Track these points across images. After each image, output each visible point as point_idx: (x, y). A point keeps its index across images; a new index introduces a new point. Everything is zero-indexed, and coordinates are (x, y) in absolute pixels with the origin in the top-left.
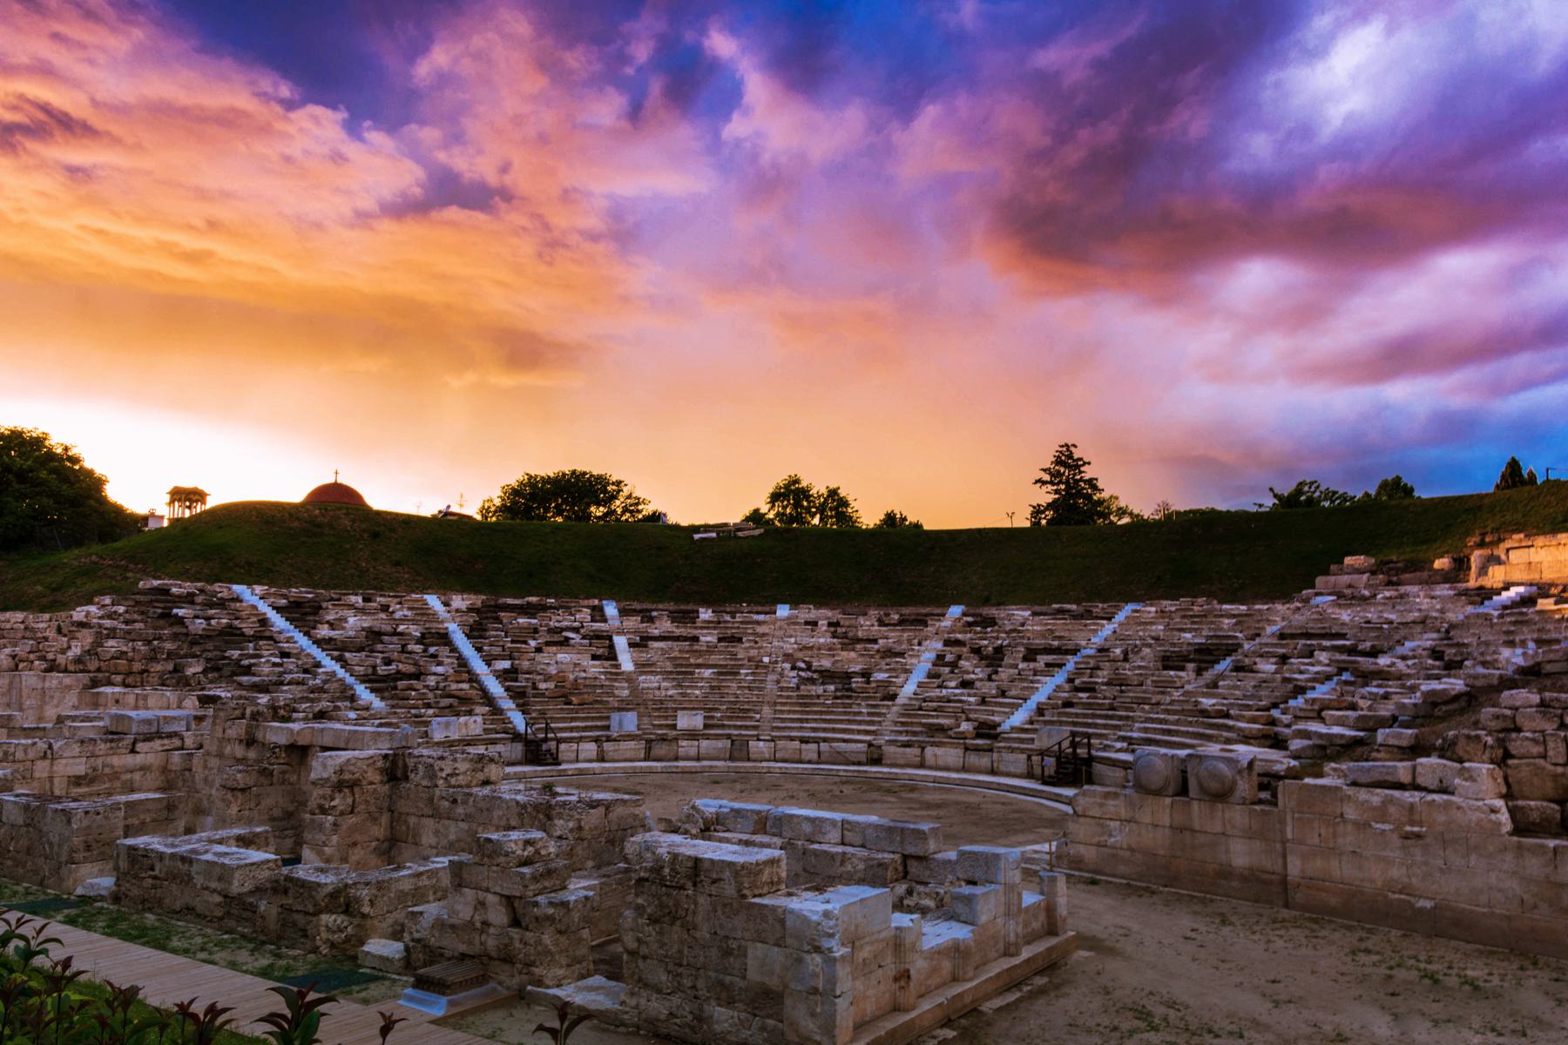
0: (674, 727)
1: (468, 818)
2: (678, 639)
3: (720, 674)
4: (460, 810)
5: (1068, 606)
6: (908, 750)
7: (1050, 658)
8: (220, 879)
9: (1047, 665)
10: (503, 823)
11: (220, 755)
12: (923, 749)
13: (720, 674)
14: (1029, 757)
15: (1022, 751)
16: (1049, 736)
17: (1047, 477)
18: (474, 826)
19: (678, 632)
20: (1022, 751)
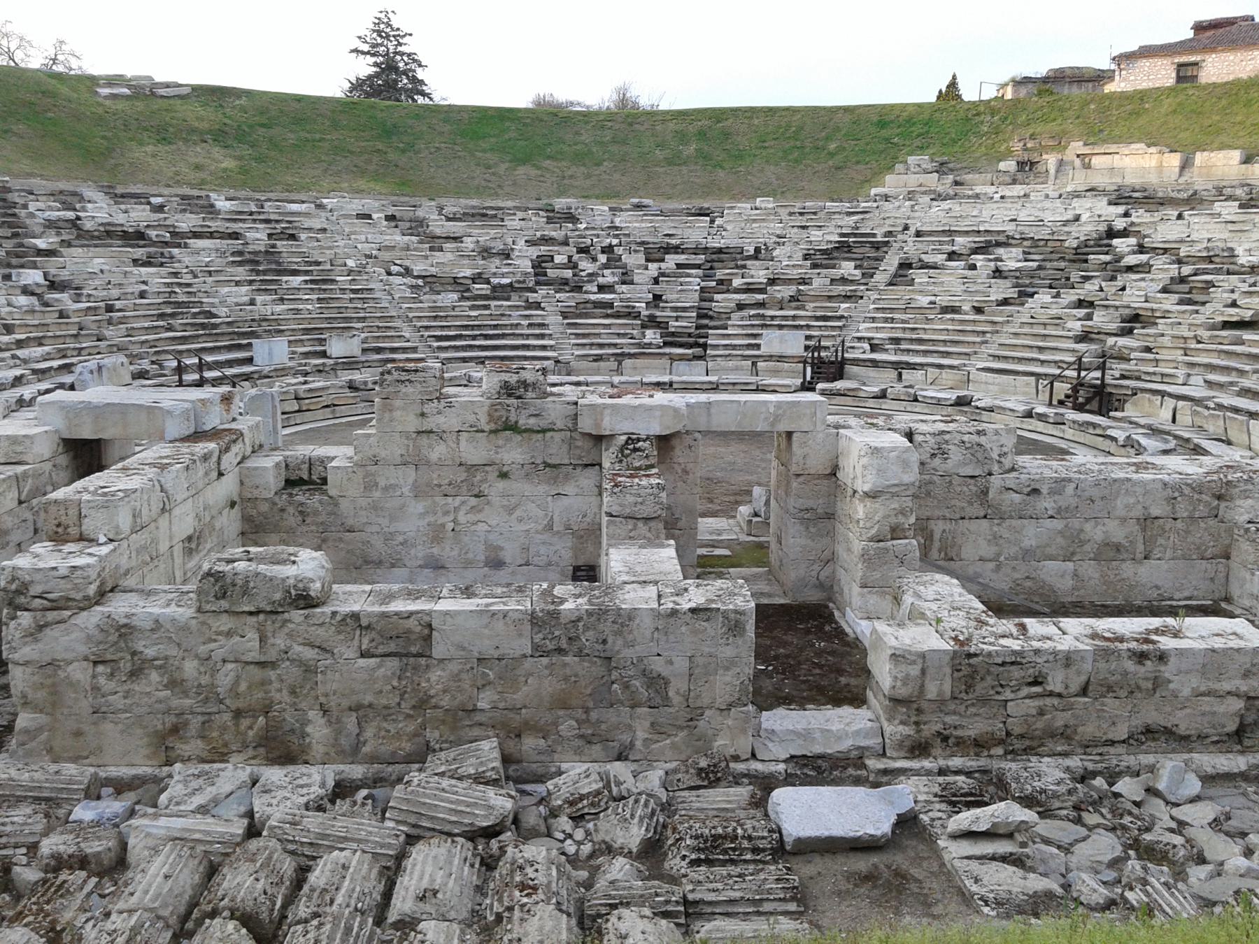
0: (323, 354)
1: (1059, 513)
2: (211, 235)
3: (312, 282)
4: (1046, 503)
5: (646, 201)
6: (602, 364)
7: (681, 258)
8: (1246, 675)
9: (679, 266)
10: (1138, 512)
11: (417, 462)
12: (620, 363)
13: (312, 282)
14: (754, 364)
15: (745, 357)
16: (782, 340)
17: (366, 48)
18: (1076, 523)
19: (215, 225)
20: (745, 357)
